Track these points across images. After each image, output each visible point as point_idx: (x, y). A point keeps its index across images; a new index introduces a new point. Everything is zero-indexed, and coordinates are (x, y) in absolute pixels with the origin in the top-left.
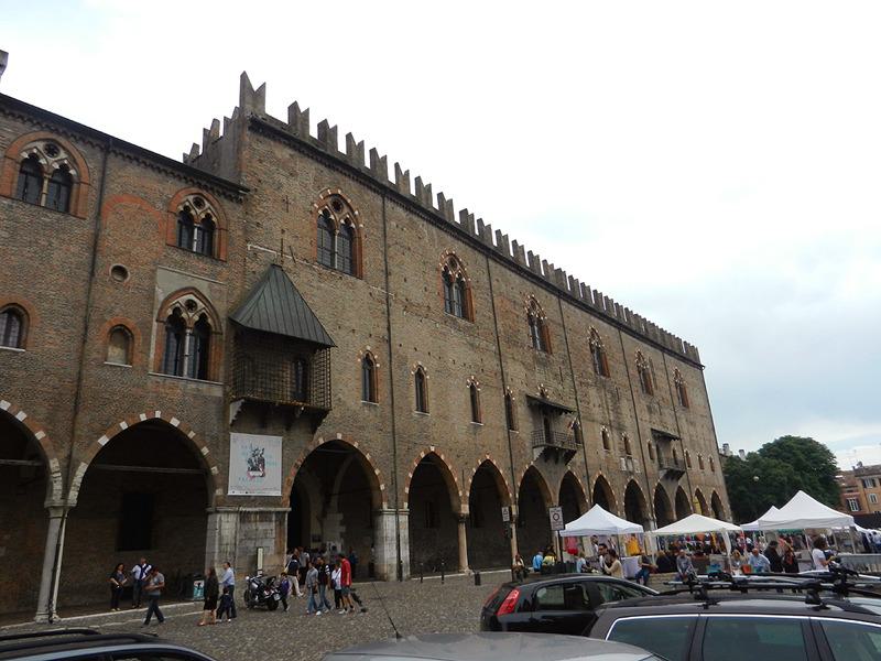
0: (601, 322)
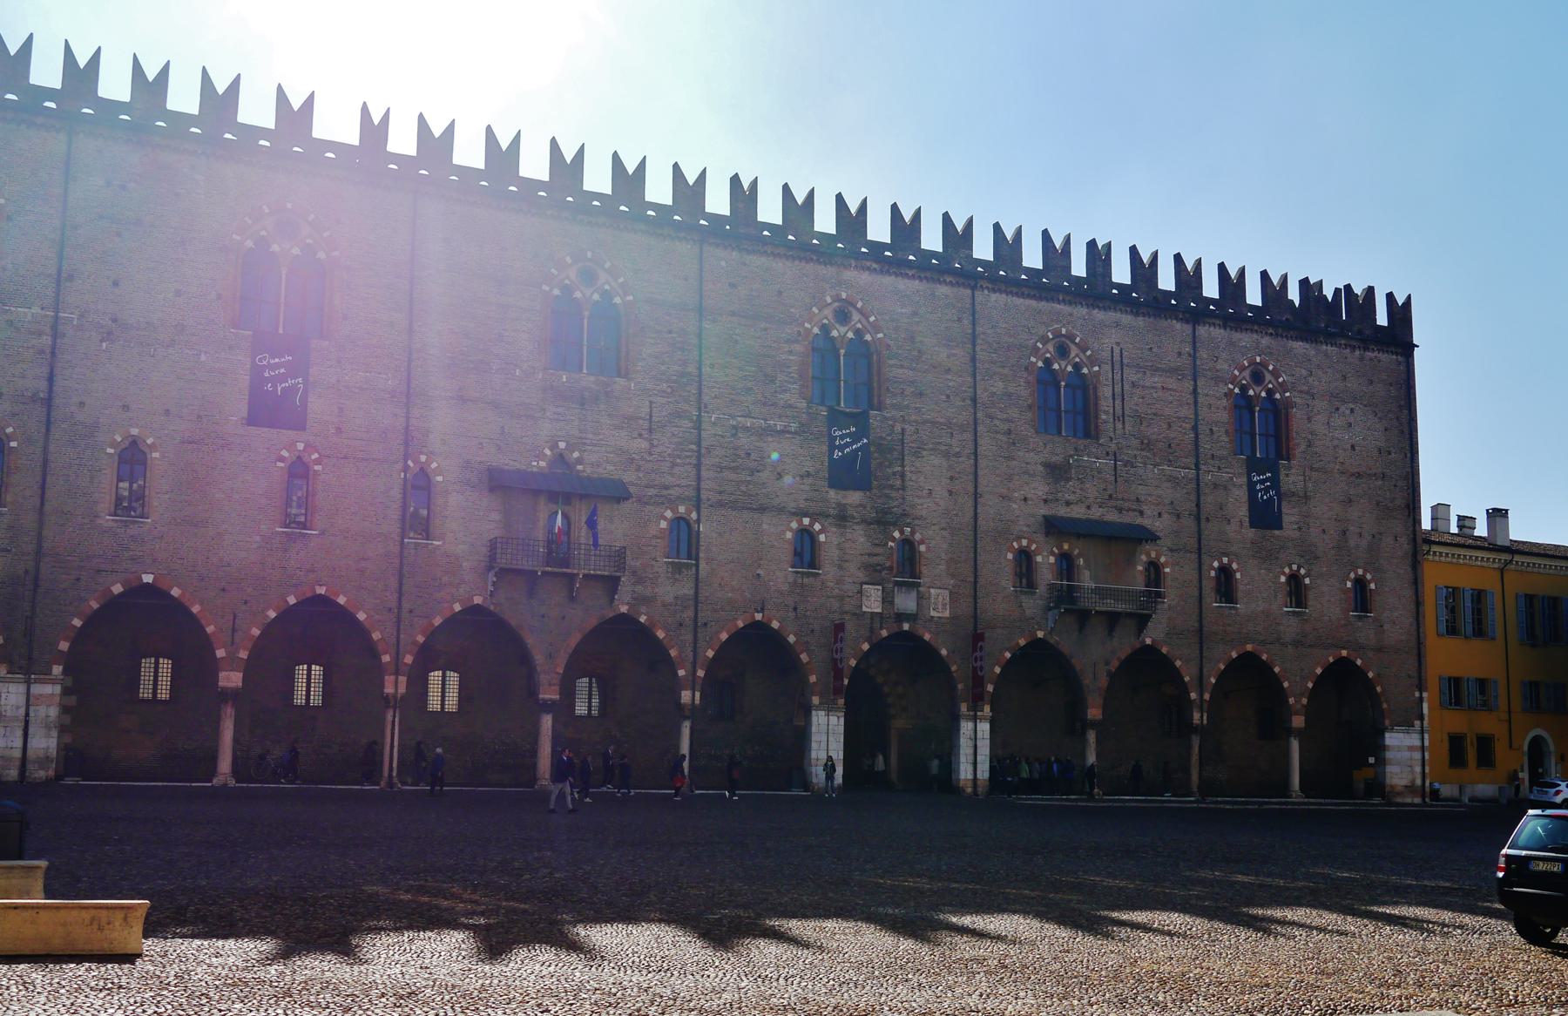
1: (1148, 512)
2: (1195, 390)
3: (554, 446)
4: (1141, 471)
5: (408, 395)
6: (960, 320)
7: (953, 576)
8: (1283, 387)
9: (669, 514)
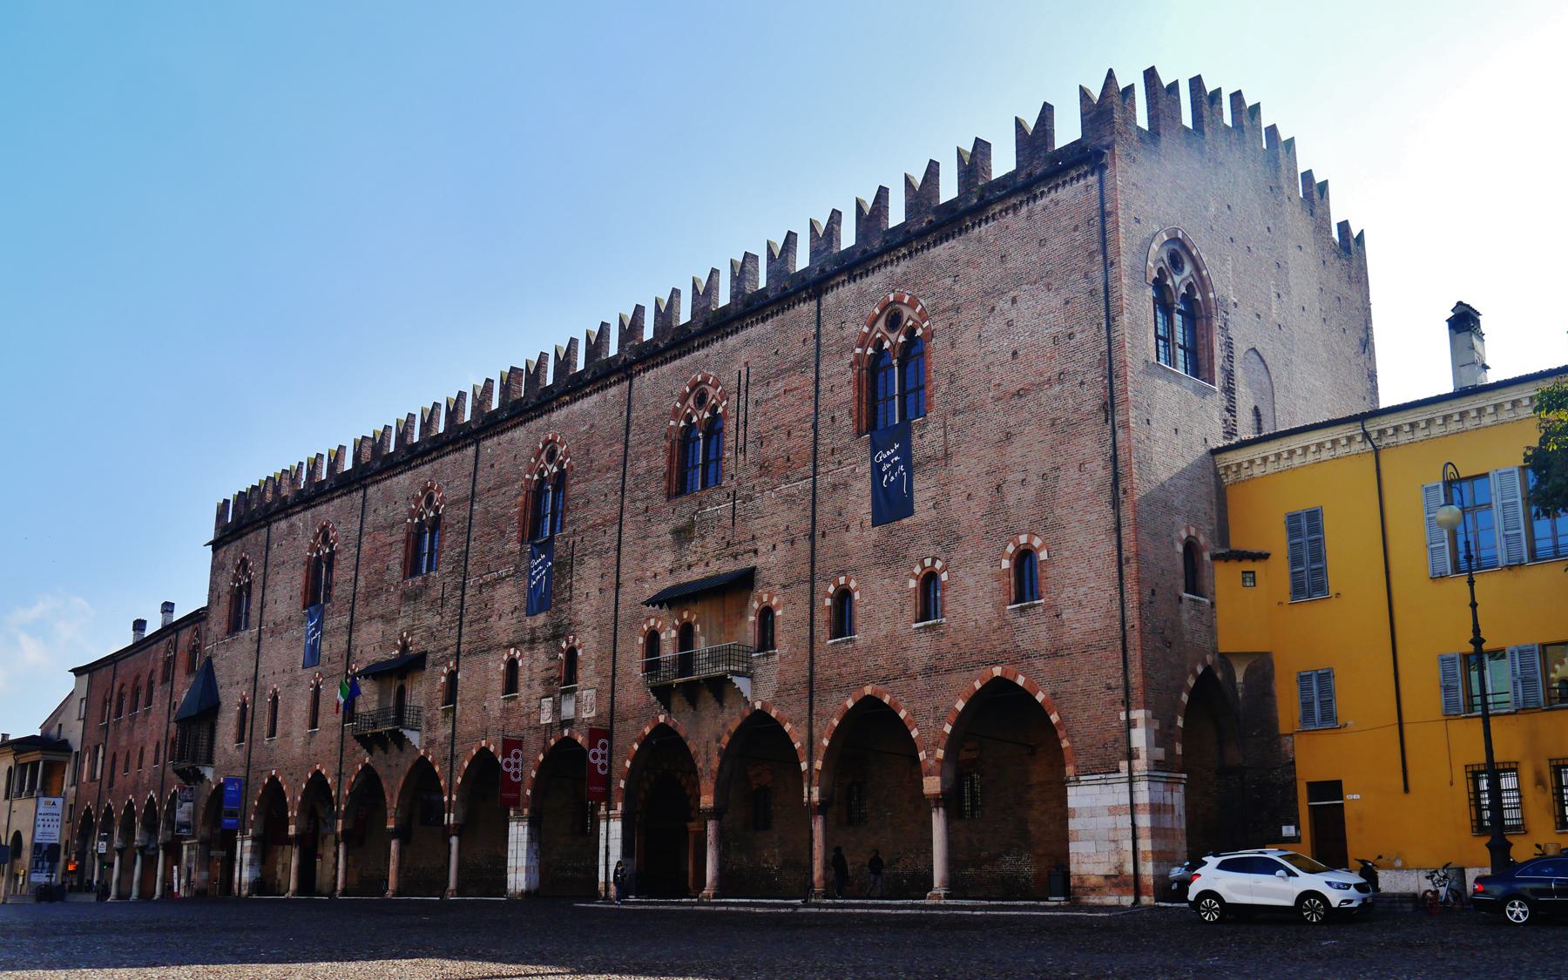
1: (762, 549)
8: (923, 316)
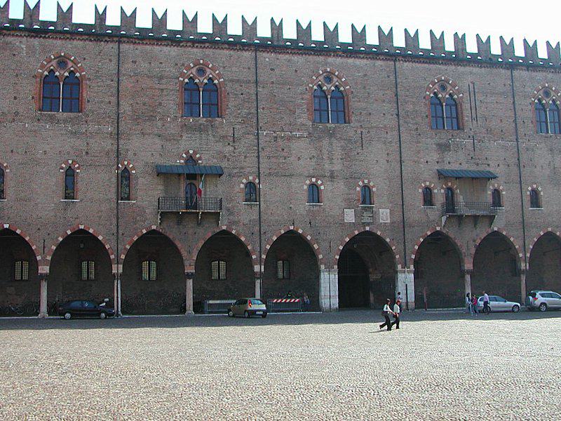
0: (350, 61)
1: (492, 165)
2: (514, 103)
3: (187, 153)
4: (488, 144)
5: (118, 134)
6: (388, 77)
7: (391, 202)
9: (244, 181)
